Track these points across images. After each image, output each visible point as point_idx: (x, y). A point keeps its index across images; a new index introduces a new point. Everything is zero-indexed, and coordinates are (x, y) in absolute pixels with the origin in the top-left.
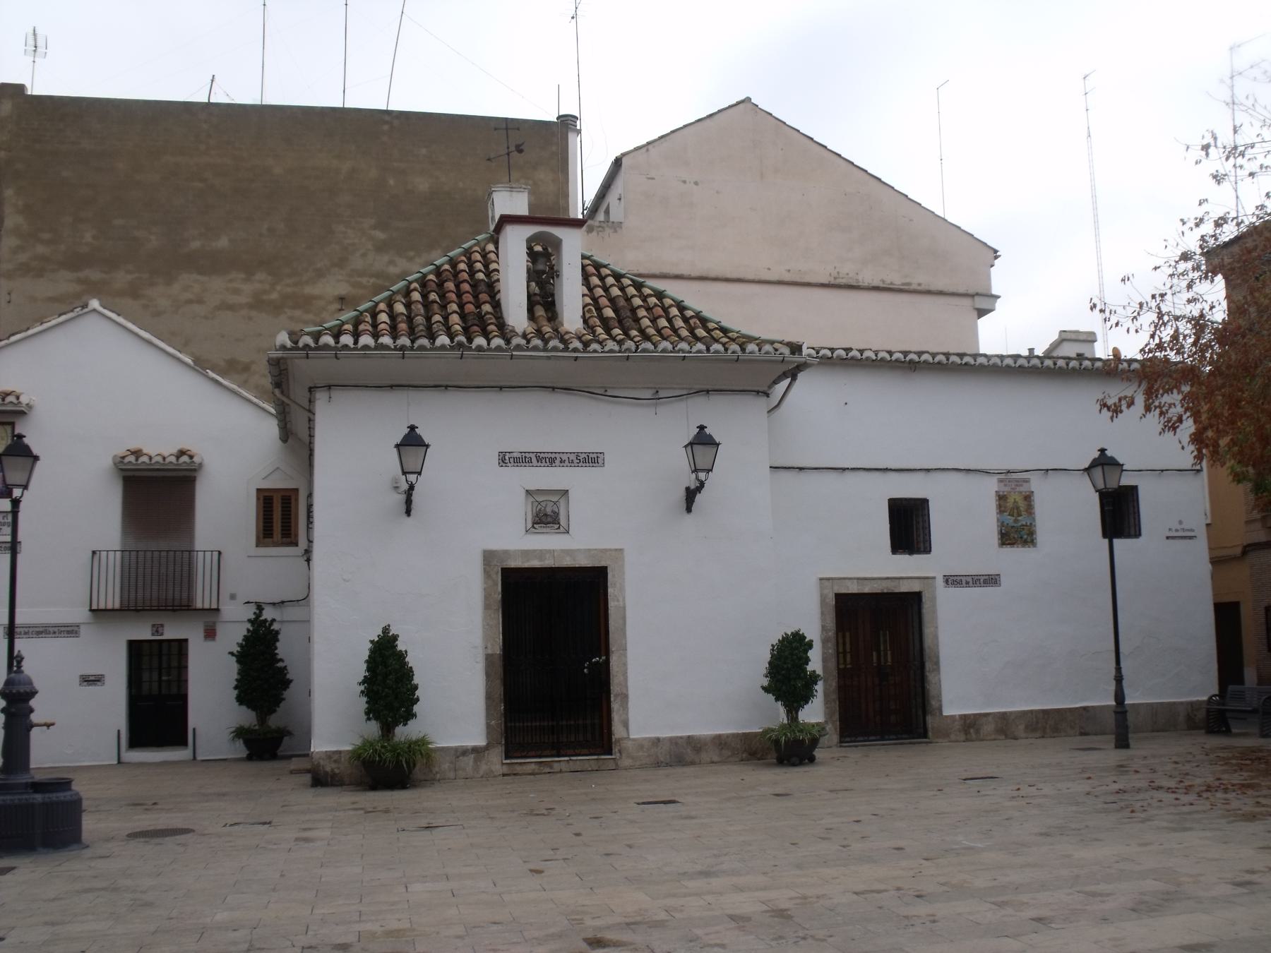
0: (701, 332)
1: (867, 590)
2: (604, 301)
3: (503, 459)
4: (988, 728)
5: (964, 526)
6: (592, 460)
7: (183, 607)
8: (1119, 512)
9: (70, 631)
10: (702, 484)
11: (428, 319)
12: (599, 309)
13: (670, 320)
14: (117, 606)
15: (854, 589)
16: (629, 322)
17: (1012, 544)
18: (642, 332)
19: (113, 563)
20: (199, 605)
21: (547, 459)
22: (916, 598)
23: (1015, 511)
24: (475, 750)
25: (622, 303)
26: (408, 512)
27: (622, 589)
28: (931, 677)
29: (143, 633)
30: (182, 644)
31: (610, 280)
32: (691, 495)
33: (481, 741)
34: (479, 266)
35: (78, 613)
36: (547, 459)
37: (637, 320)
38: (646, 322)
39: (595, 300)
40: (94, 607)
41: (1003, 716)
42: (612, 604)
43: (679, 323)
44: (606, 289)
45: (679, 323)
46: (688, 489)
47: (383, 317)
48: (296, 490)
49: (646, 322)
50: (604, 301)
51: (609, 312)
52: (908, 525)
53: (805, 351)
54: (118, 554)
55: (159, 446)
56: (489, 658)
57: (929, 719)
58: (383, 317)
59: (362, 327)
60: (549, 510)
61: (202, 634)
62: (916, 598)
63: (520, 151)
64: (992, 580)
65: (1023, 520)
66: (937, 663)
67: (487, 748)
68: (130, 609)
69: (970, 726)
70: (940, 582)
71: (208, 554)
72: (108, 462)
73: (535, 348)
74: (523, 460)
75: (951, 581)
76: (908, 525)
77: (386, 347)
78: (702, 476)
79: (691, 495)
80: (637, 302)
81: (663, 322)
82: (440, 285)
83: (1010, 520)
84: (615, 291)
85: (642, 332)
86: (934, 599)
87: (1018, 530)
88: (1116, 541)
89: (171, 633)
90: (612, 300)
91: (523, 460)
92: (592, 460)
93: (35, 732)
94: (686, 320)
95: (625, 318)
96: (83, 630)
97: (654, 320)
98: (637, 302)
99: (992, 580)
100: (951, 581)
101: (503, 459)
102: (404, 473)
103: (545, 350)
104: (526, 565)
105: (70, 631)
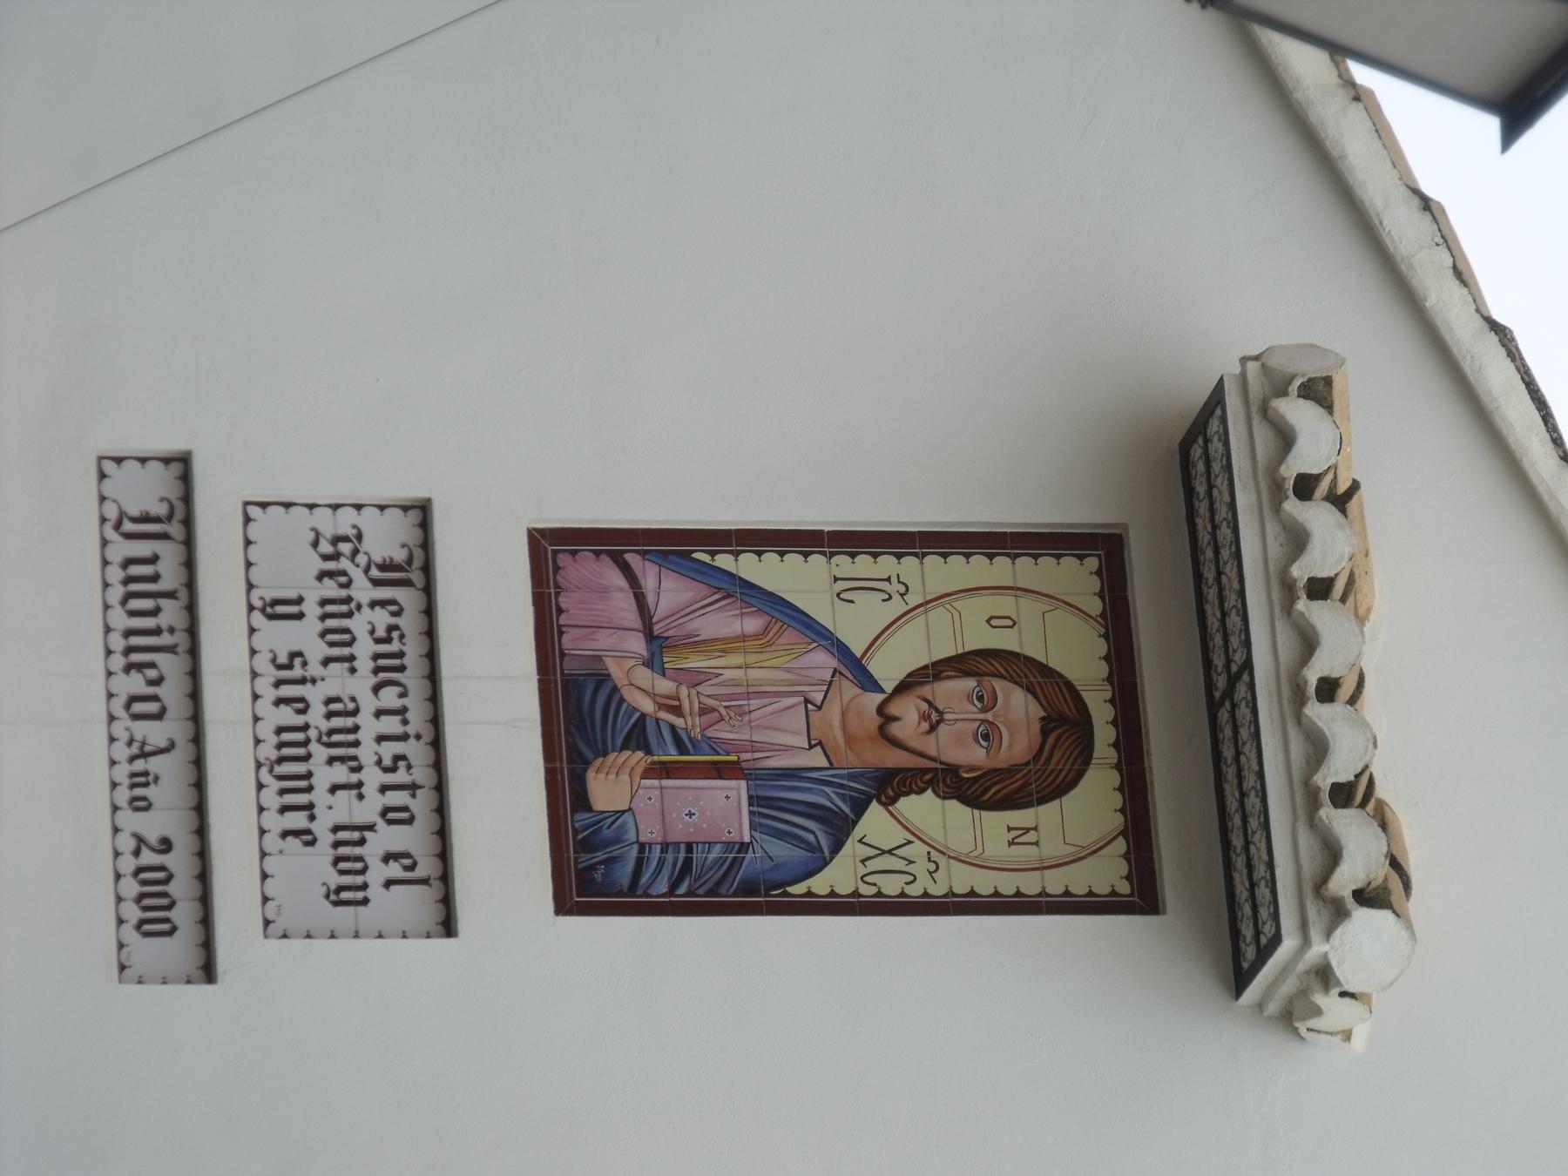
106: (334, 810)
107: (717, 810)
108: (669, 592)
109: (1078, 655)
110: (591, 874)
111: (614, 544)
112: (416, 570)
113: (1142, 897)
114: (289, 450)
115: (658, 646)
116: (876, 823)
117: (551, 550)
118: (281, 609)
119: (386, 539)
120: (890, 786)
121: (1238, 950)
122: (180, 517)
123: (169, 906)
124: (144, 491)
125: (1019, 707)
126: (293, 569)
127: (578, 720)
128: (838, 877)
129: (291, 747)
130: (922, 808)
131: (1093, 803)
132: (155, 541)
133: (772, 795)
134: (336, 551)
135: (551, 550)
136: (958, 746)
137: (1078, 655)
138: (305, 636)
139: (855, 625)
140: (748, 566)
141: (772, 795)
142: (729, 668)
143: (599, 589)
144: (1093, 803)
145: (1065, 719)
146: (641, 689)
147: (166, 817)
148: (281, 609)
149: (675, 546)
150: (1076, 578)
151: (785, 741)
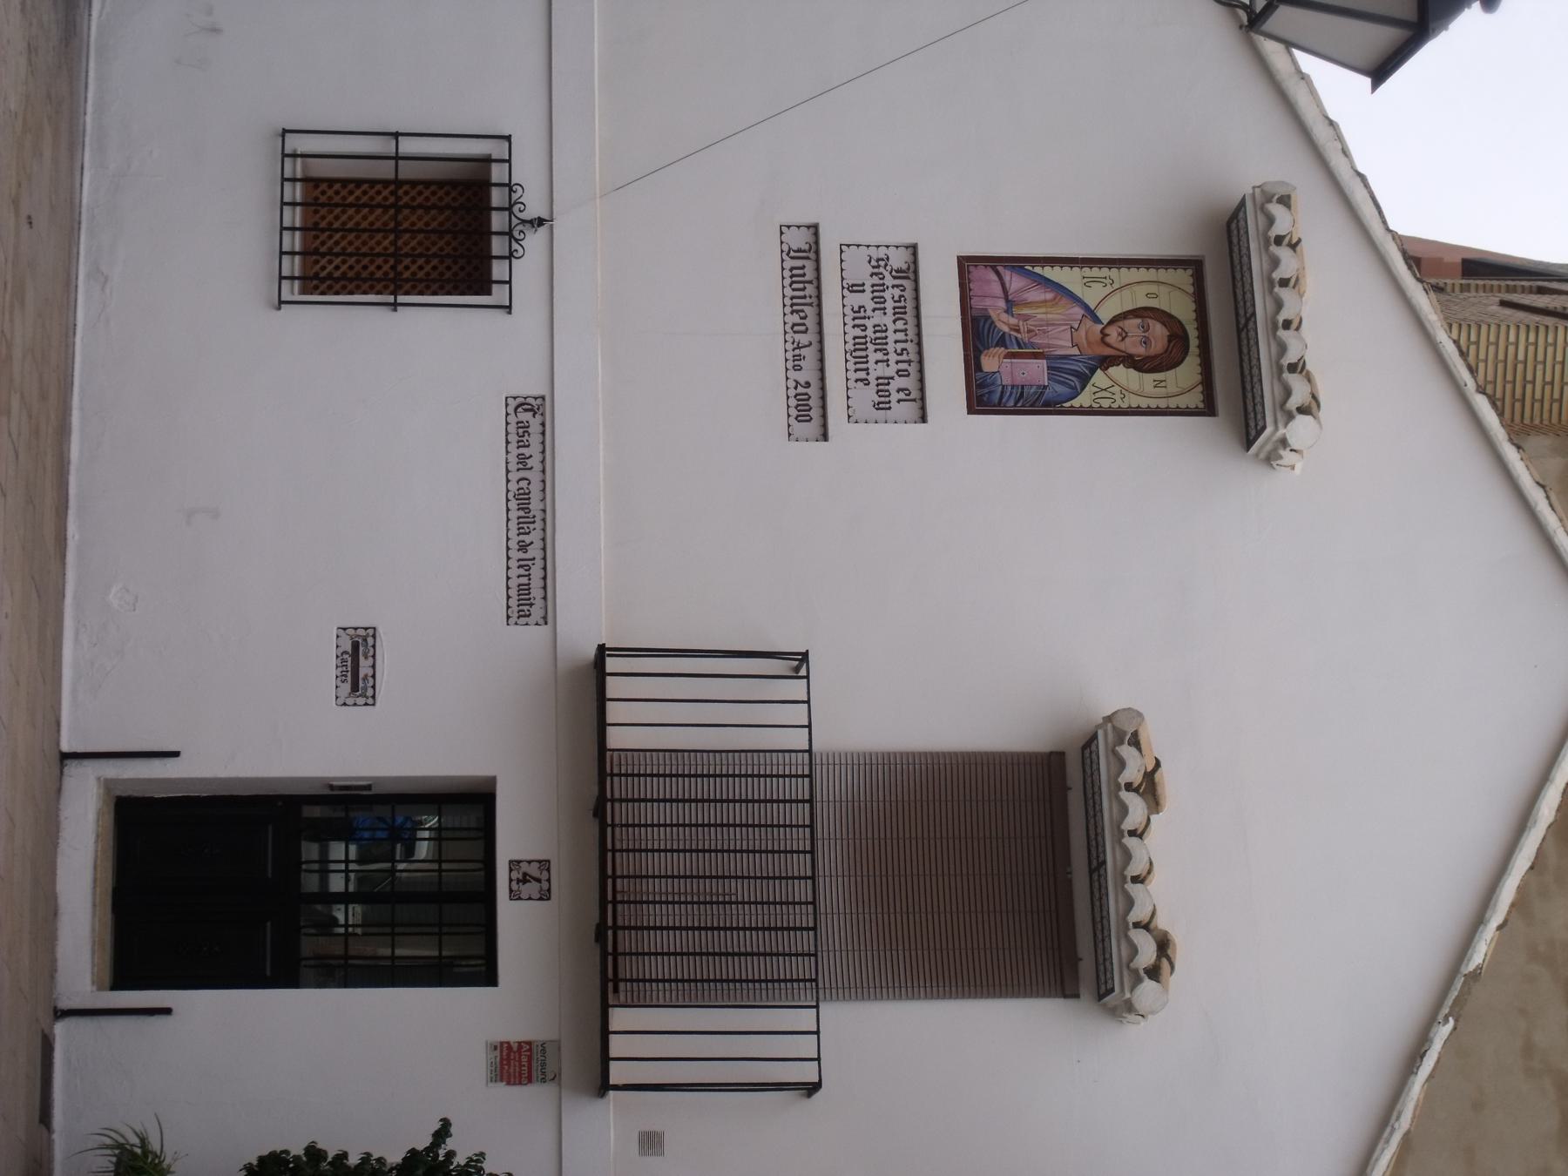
7: (613, 964)
9: (529, 596)
14: (617, 738)
19: (765, 725)
20: (620, 1018)
29: (518, 834)
30: (481, 969)
35: (585, 617)
40: (612, 664)
54: (798, 740)
55: (1176, 867)
61: (515, 1035)
68: (605, 786)
71: (806, 1046)
72: (1108, 700)
89: (519, 926)
96: (532, 636)
105: (529, 596)
106: (878, 370)
107: (1034, 372)
108: (1015, 282)
109: (1183, 310)
110: (983, 397)
112: (911, 273)
113: (1208, 409)
114: (858, 223)
115: (1010, 304)
116: (1099, 378)
117: (966, 265)
118: (855, 288)
119: (899, 260)
120: (1105, 362)
121: (1248, 432)
122: (813, 251)
123: (809, 410)
124: (799, 240)
125: (1159, 331)
126: (860, 271)
127: (978, 333)
128: (1084, 400)
129: (860, 345)
130: (1119, 372)
131: (1188, 372)
132: (804, 260)
133: (1057, 365)
134: (878, 265)
135: (966, 265)
136: (1134, 347)
137: (1183, 310)
138: (865, 299)
139: (1091, 296)
140: (1048, 272)
141: (1057, 365)
142: (1040, 314)
143: (987, 282)
144: (1188, 372)
145: (1178, 336)
146: (1003, 322)
147: (808, 374)
148: (855, 288)
149: (1018, 264)
150: (1183, 277)
151: (1062, 344)
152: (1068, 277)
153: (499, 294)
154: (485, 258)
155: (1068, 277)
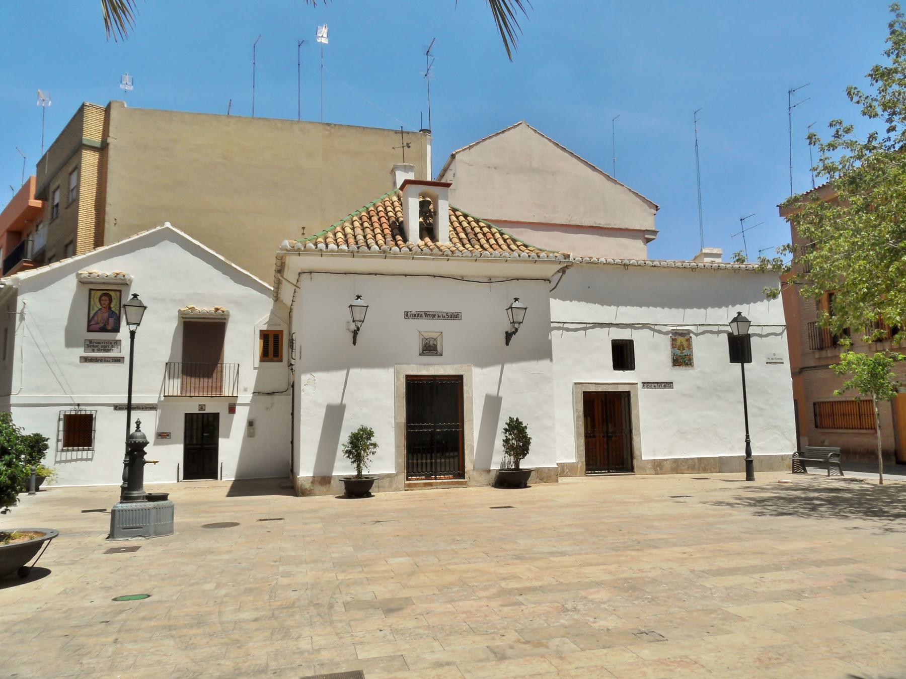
0: (513, 247)
1: (600, 390)
2: (459, 229)
3: (407, 315)
4: (668, 466)
5: (651, 356)
6: (455, 316)
8: (740, 349)
10: (517, 330)
11: (365, 237)
12: (457, 234)
13: (496, 240)
15: (593, 389)
16: (474, 241)
17: (680, 365)
18: (482, 246)
21: (432, 316)
22: (628, 394)
23: (681, 347)
24: (389, 476)
25: (469, 230)
26: (354, 343)
27: (471, 387)
28: (635, 437)
31: (462, 218)
32: (508, 336)
33: (393, 471)
34: (389, 209)
36: (432, 316)
37: (478, 240)
38: (483, 241)
39: (455, 229)
41: (676, 461)
42: (465, 395)
43: (501, 242)
44: (460, 223)
45: (501, 242)
46: (507, 333)
47: (340, 235)
48: (282, 331)
49: (483, 241)
50: (459, 229)
51: (463, 235)
52: (623, 356)
53: (571, 258)
56: (397, 425)
57: (635, 462)
58: (340, 235)
59: (328, 240)
60: (431, 343)
62: (628, 394)
63: (409, 147)
64: (669, 385)
65: (685, 352)
66: (639, 430)
67: (396, 475)
69: (658, 467)
70: (640, 386)
73: (425, 254)
74: (417, 316)
75: (646, 385)
76: (623, 356)
77: (343, 251)
78: (516, 325)
79: (508, 336)
80: (477, 230)
81: (492, 241)
82: (370, 219)
83: (678, 352)
84: (465, 224)
85: (482, 246)
86: (637, 395)
87: (683, 357)
88: (745, 364)
90: (464, 229)
91: (417, 316)
92: (455, 316)
93: (146, 466)
94: (505, 240)
95: (471, 237)
97: (487, 241)
98: (477, 230)
99: (669, 385)
100: (646, 385)
101: (407, 315)
102: (354, 321)
103: (431, 255)
104: (419, 373)
107: (111, 320)
108: (93, 322)
111: (89, 326)
112: (91, 341)
115: (97, 323)
117: (89, 330)
120: (110, 308)
125: (103, 298)
127: (103, 330)
128: (117, 312)
130: (112, 305)
133: (110, 316)
135: (89, 330)
136: (107, 303)
137: (100, 293)
140: (91, 315)
141: (110, 316)
143: (91, 327)
145: (106, 295)
146: (101, 325)
149: (89, 321)
150: (93, 292)
151: (106, 315)
152: (92, 313)
153: (94, 413)
154: (86, 415)
155: (92, 313)
